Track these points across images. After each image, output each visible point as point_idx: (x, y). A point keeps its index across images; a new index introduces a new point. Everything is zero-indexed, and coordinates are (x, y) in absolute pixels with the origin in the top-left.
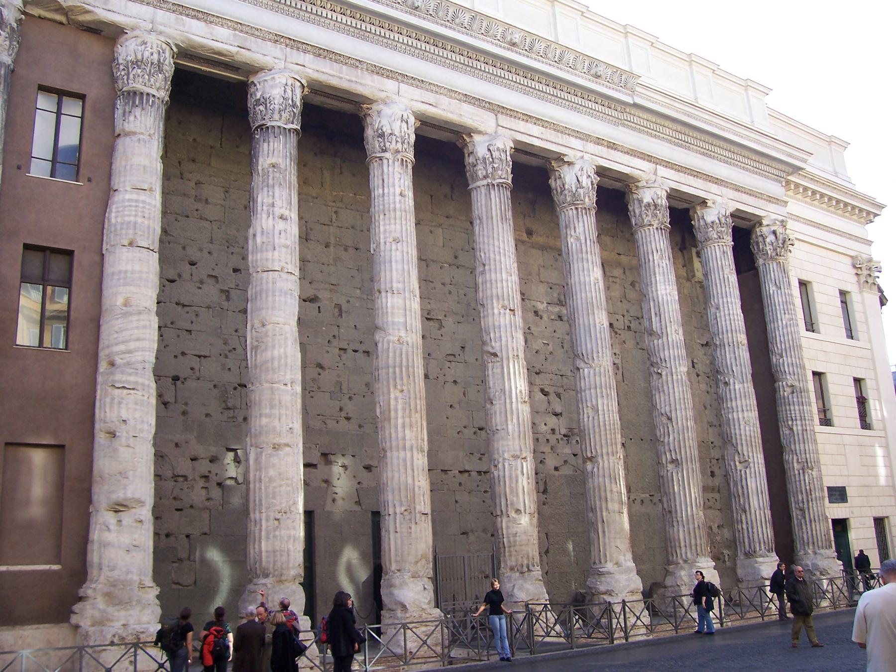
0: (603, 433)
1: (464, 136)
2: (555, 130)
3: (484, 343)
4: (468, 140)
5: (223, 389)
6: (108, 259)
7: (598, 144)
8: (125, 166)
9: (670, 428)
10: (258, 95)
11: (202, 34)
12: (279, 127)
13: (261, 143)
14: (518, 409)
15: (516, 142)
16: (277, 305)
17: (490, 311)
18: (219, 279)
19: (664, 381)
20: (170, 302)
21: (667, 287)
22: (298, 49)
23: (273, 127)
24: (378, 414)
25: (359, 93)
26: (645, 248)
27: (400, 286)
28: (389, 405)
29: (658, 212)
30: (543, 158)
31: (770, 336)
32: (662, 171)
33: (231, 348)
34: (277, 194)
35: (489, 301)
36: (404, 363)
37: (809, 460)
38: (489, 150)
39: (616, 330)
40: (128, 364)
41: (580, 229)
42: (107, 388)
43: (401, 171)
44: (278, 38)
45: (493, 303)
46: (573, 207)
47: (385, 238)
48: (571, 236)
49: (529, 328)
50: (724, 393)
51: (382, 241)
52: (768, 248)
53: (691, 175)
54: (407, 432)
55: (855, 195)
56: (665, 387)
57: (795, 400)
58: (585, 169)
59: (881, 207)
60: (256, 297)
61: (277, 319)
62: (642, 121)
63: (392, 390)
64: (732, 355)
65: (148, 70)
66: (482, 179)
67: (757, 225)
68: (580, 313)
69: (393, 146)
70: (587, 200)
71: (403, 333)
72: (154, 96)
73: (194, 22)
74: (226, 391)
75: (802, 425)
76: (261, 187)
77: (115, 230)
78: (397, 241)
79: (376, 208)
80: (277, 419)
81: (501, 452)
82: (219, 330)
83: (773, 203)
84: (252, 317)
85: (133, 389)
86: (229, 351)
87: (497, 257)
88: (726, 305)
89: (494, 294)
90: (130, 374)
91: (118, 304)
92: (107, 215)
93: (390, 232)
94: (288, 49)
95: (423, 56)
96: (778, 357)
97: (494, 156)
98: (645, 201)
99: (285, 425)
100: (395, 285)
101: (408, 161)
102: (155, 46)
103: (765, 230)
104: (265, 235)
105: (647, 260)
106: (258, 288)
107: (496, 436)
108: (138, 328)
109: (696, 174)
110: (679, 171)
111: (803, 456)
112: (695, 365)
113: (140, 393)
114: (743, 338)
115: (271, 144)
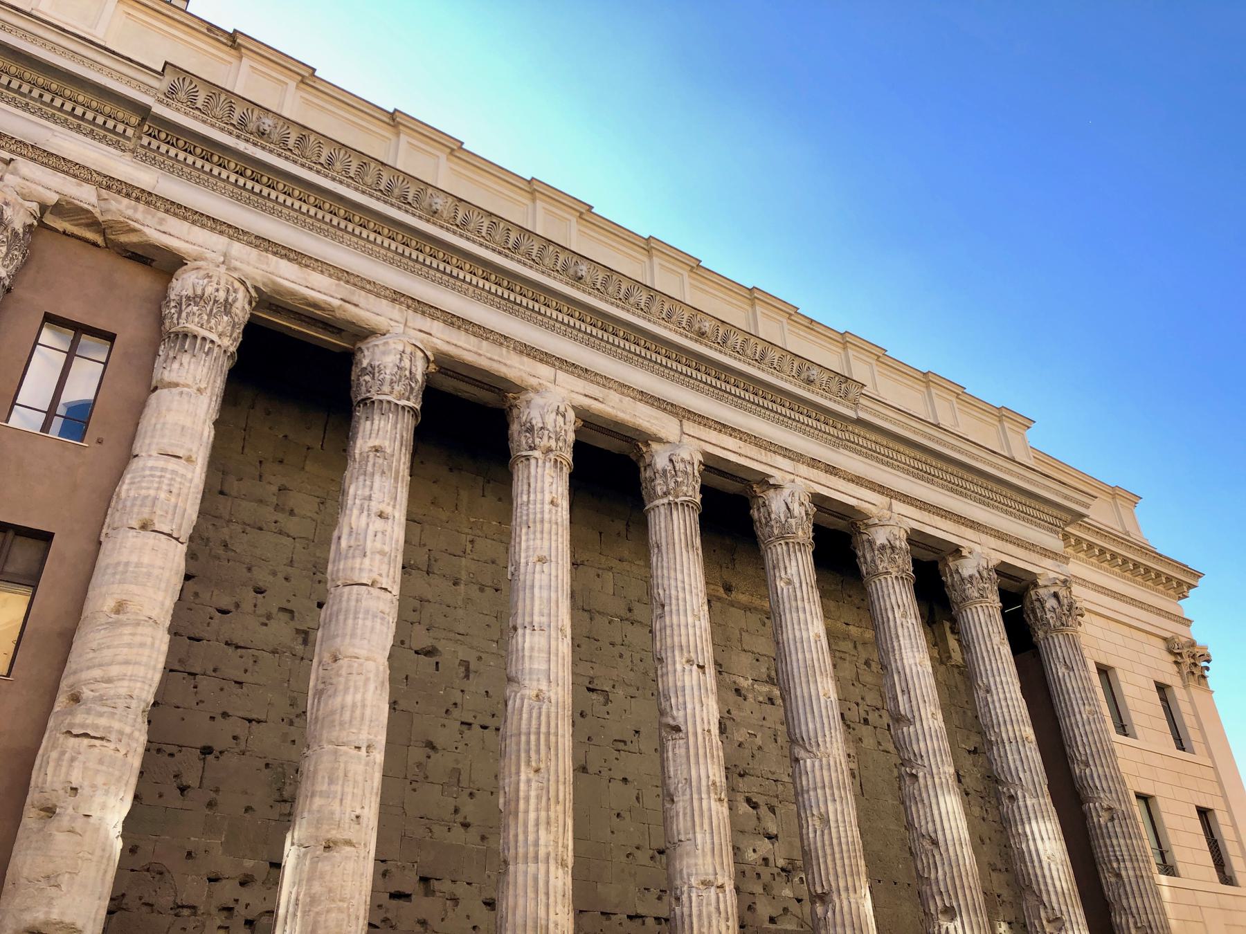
0: (837, 856)
1: (640, 444)
2: (756, 445)
3: (662, 713)
4: (644, 449)
5: (280, 770)
6: (107, 546)
7: (813, 467)
8: (155, 424)
9: (937, 857)
10: (365, 363)
11: (293, 278)
12: (389, 402)
13: (362, 421)
14: (710, 809)
15: (706, 454)
16: (359, 632)
17: (670, 668)
18: (296, 614)
19: (922, 785)
20: (217, 640)
21: (916, 654)
22: (423, 313)
23: (381, 401)
24: (501, 806)
25: (502, 375)
26: (882, 604)
27: (545, 619)
28: (517, 790)
29: (897, 557)
30: (742, 480)
31: (1065, 737)
32: (899, 507)
33: (299, 711)
34: (377, 485)
35: (669, 654)
36: (543, 729)
37: (1153, 924)
38: (671, 460)
39: (849, 723)
40: (101, 699)
41: (792, 570)
42: (58, 735)
43: (554, 475)
44: (397, 297)
45: (674, 656)
46: (782, 542)
47: (527, 557)
48: (781, 579)
49: (729, 712)
50: (1010, 812)
51: (523, 561)
52: (1048, 616)
53: (938, 515)
54: (542, 833)
55: (1160, 557)
56: (924, 795)
57: (1118, 829)
58: (796, 495)
59: (1197, 575)
60: (330, 621)
61: (356, 651)
62: (869, 443)
63: (523, 768)
64: (1017, 757)
65: (208, 309)
66: (662, 497)
67: (1032, 587)
68: (797, 680)
69: (545, 443)
70: (800, 533)
71: (544, 686)
72: (212, 342)
73: (284, 263)
74: (284, 775)
75: (1134, 869)
76: (356, 474)
77: (124, 507)
78: (542, 560)
79: (518, 520)
80: (338, 801)
81: (685, 877)
82: (286, 685)
83: (1049, 557)
84: (321, 648)
85: (102, 739)
86: (297, 716)
87: (681, 595)
88: (999, 686)
89: (676, 644)
90: (101, 715)
91: (105, 609)
92: (117, 489)
93: (535, 550)
94: (410, 312)
95: (589, 341)
96: (1082, 767)
97: (677, 468)
98: (878, 543)
99: (348, 810)
100: (536, 619)
101: (564, 462)
102: (223, 282)
103: (1041, 591)
104: (354, 535)
105: (885, 620)
106: (335, 608)
107: (679, 850)
108: (130, 645)
109: (943, 513)
110: (920, 508)
111: (1144, 917)
112: (963, 780)
113: (112, 746)
114: (1029, 732)
115: (376, 422)
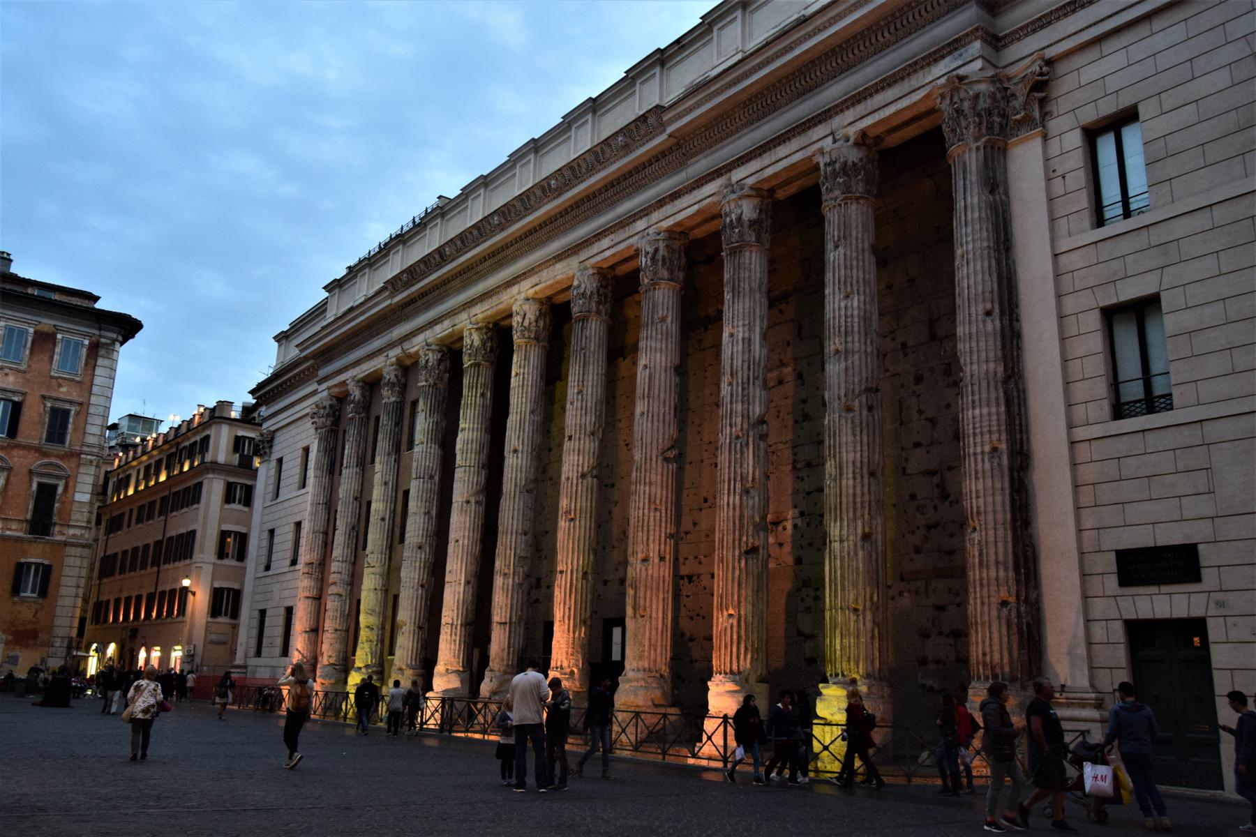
2: (621, 228)
7: (662, 206)
32: (737, 175)
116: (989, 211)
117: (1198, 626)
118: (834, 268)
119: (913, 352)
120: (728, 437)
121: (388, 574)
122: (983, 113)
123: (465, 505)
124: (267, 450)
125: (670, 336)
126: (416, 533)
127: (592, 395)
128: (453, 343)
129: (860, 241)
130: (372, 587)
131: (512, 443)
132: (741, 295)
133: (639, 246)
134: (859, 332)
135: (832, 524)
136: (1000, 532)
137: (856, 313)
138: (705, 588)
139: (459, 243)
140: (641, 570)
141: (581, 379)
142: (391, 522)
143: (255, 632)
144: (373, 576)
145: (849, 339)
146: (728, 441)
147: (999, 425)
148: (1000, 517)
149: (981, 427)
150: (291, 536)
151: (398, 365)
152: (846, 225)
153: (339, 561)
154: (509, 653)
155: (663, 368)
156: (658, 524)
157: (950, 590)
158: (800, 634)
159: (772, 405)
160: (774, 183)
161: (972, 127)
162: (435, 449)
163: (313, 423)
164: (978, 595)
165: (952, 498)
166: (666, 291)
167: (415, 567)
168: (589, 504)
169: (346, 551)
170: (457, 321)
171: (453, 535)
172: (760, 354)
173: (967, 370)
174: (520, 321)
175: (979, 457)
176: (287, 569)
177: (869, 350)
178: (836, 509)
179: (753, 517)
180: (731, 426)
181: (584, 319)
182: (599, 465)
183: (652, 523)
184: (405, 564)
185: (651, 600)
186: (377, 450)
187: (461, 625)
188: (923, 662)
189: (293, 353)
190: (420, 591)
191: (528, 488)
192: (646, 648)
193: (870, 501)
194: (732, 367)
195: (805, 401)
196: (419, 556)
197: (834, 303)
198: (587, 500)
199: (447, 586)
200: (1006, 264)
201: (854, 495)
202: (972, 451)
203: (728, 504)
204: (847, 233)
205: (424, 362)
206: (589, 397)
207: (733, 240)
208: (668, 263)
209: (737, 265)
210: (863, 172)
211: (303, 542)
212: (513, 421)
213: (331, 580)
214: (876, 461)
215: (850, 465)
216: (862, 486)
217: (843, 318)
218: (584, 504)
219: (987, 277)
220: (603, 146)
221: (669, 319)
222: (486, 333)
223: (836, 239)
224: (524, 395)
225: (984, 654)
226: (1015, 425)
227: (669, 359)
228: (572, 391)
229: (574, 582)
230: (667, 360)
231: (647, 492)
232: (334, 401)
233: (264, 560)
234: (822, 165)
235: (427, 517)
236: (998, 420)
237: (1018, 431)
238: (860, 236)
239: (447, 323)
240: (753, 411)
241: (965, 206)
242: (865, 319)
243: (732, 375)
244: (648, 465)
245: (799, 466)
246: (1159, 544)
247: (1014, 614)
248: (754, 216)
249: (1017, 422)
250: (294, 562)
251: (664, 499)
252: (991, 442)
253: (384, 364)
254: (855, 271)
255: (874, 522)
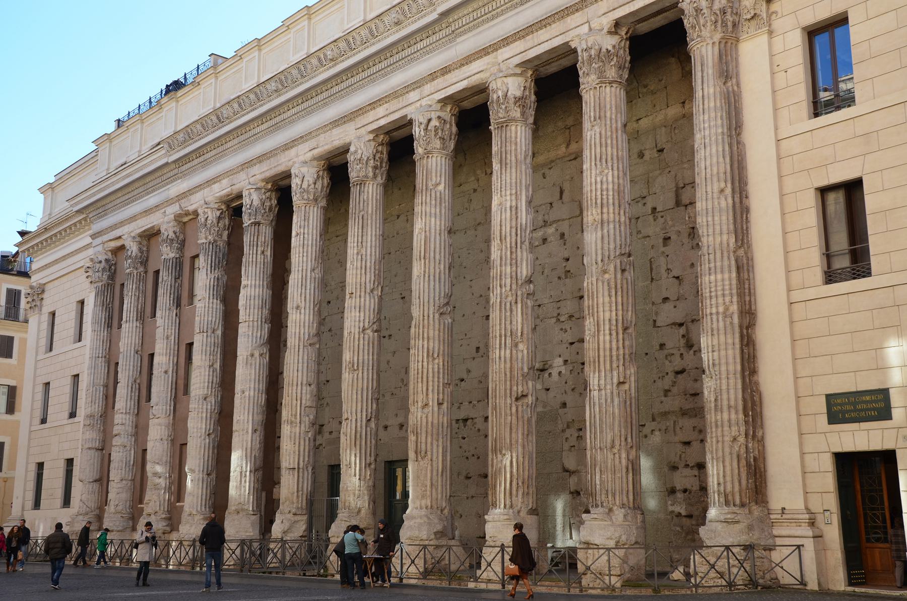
7: (433, 80)
32: (505, 53)
53: (541, 29)
95: (309, 112)
110: (523, 37)
116: (723, 101)
117: (888, 458)
118: (591, 145)
119: (662, 217)
120: (498, 296)
121: (174, 424)
122: (718, 12)
123: (250, 358)
124: (38, 303)
125: (443, 201)
126: (202, 385)
127: (371, 255)
128: (233, 200)
129: (614, 121)
130: (158, 437)
131: (295, 300)
132: (508, 166)
133: (413, 117)
134: (613, 204)
135: (591, 376)
136: (732, 381)
137: (611, 186)
138: (479, 430)
139: (236, 106)
140: (421, 417)
141: (360, 240)
142: (175, 374)
143: (31, 485)
144: (159, 427)
145: (605, 210)
146: (498, 300)
147: (731, 289)
148: (731, 368)
149: (716, 291)
150: (68, 389)
151: (175, 220)
152: (601, 107)
153: (122, 413)
154: (298, 497)
155: (438, 232)
156: (436, 375)
157: (694, 427)
158: (566, 470)
159: (538, 262)
160: (536, 63)
161: (709, 24)
162: (217, 305)
163: (87, 277)
164: (714, 435)
165: (695, 348)
166: (439, 158)
167: (202, 417)
168: (371, 357)
169: (129, 403)
170: (235, 181)
171: (238, 387)
172: (526, 219)
173: (704, 240)
174: (299, 183)
175: (714, 317)
176: (66, 422)
177: (623, 219)
178: (594, 362)
179: (522, 369)
180: (501, 286)
181: (362, 183)
182: (379, 320)
183: (431, 375)
184: (191, 415)
185: (432, 444)
186: (158, 305)
187: (251, 471)
188: (672, 491)
189: (62, 206)
190: (207, 441)
191: (311, 342)
192: (428, 488)
193: (624, 354)
194: (501, 233)
195: (568, 260)
196: (205, 407)
197: (591, 178)
198: (368, 354)
199: (235, 435)
200: (738, 148)
201: (611, 349)
202: (708, 312)
203: (500, 358)
204: (602, 114)
205: (203, 220)
206: (368, 257)
207: (500, 115)
208: (440, 134)
209: (503, 139)
210: (615, 59)
211: (82, 394)
212: (294, 280)
213: (115, 432)
214: (629, 318)
215: (607, 322)
216: (618, 341)
217: (599, 193)
218: (366, 357)
219: (721, 159)
220: (377, 21)
221: (441, 187)
222: (265, 193)
223: (592, 119)
224: (305, 254)
225: (719, 484)
226: (744, 289)
227: (443, 223)
228: (351, 251)
229: (359, 429)
230: (441, 224)
231: (426, 346)
232: (110, 255)
233: (38, 415)
234: (579, 50)
235: (211, 370)
236: (730, 284)
237: (747, 294)
238: (614, 117)
239: (225, 182)
240: (521, 272)
241: (703, 96)
242: (619, 192)
243: (501, 240)
244: (426, 322)
245: (562, 319)
246: (859, 390)
247: (743, 450)
248: (518, 94)
249: (747, 286)
250: (73, 415)
251: (441, 352)
252: (724, 303)
253: (165, 221)
254: (609, 149)
255: (628, 372)
